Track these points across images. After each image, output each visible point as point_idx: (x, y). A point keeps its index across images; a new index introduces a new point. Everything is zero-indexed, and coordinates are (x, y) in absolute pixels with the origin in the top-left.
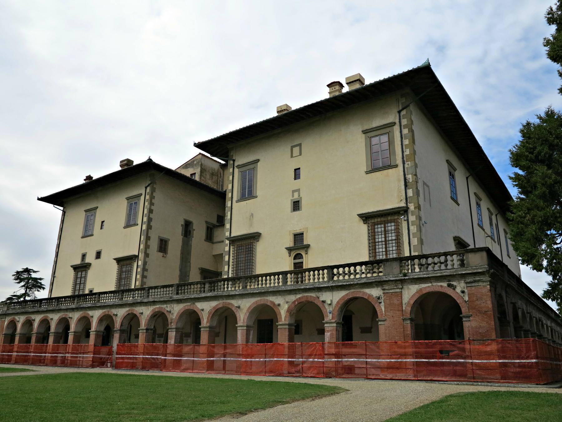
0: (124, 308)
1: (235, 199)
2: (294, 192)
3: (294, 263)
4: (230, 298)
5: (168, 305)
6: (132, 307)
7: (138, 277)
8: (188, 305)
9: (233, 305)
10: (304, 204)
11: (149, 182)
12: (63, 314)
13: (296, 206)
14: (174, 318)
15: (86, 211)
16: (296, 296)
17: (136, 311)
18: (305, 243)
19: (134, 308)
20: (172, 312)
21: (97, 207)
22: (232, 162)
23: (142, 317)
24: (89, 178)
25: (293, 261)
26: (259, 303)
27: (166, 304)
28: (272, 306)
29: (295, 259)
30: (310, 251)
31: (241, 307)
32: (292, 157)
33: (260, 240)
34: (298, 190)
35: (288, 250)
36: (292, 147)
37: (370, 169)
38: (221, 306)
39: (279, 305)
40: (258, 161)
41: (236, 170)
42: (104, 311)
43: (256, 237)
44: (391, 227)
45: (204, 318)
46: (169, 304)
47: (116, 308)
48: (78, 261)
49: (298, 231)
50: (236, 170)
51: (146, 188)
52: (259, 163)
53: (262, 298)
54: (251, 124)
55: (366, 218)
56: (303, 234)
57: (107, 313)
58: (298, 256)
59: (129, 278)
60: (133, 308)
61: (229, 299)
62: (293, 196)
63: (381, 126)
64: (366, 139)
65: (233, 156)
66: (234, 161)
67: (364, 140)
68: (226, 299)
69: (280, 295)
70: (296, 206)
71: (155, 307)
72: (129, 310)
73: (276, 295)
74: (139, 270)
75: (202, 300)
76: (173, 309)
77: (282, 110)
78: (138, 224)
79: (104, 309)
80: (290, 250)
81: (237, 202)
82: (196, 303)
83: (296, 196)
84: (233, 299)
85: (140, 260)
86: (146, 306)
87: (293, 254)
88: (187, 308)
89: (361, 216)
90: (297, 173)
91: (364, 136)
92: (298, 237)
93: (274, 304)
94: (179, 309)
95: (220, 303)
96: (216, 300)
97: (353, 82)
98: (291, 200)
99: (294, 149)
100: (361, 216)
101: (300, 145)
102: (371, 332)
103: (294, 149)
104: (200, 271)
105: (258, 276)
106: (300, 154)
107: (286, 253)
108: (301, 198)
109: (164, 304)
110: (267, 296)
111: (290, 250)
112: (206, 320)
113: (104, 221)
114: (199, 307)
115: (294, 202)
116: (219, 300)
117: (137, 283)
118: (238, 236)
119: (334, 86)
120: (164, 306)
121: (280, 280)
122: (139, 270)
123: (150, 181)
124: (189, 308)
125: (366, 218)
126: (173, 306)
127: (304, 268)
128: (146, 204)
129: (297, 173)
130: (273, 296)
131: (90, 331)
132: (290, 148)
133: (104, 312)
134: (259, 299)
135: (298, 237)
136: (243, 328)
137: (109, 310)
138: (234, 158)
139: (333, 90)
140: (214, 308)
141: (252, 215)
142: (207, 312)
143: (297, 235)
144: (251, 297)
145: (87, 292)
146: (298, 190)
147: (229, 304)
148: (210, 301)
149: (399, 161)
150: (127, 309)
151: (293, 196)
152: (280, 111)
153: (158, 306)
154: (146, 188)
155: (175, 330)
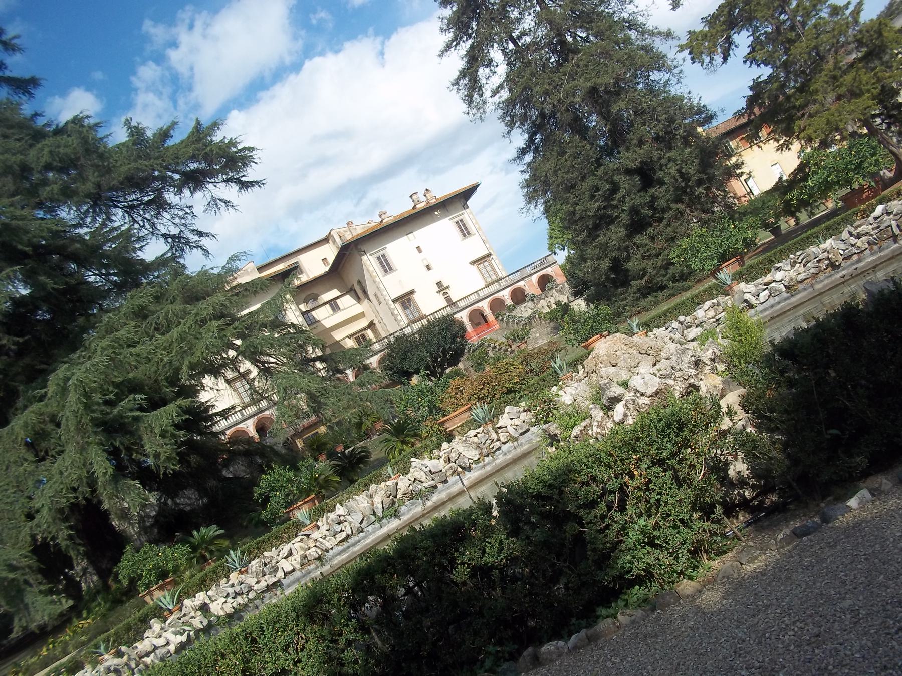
1: (380, 275)
2: (423, 260)
10: (432, 265)
13: (428, 268)
18: (445, 286)
32: (410, 240)
43: (412, 292)
44: (486, 264)
55: (473, 263)
70: (428, 268)
80: (438, 292)
81: (384, 276)
89: (471, 264)
92: (439, 284)
100: (471, 264)
125: (473, 263)
135: (439, 284)
141: (400, 281)
146: (425, 259)
149: (476, 232)
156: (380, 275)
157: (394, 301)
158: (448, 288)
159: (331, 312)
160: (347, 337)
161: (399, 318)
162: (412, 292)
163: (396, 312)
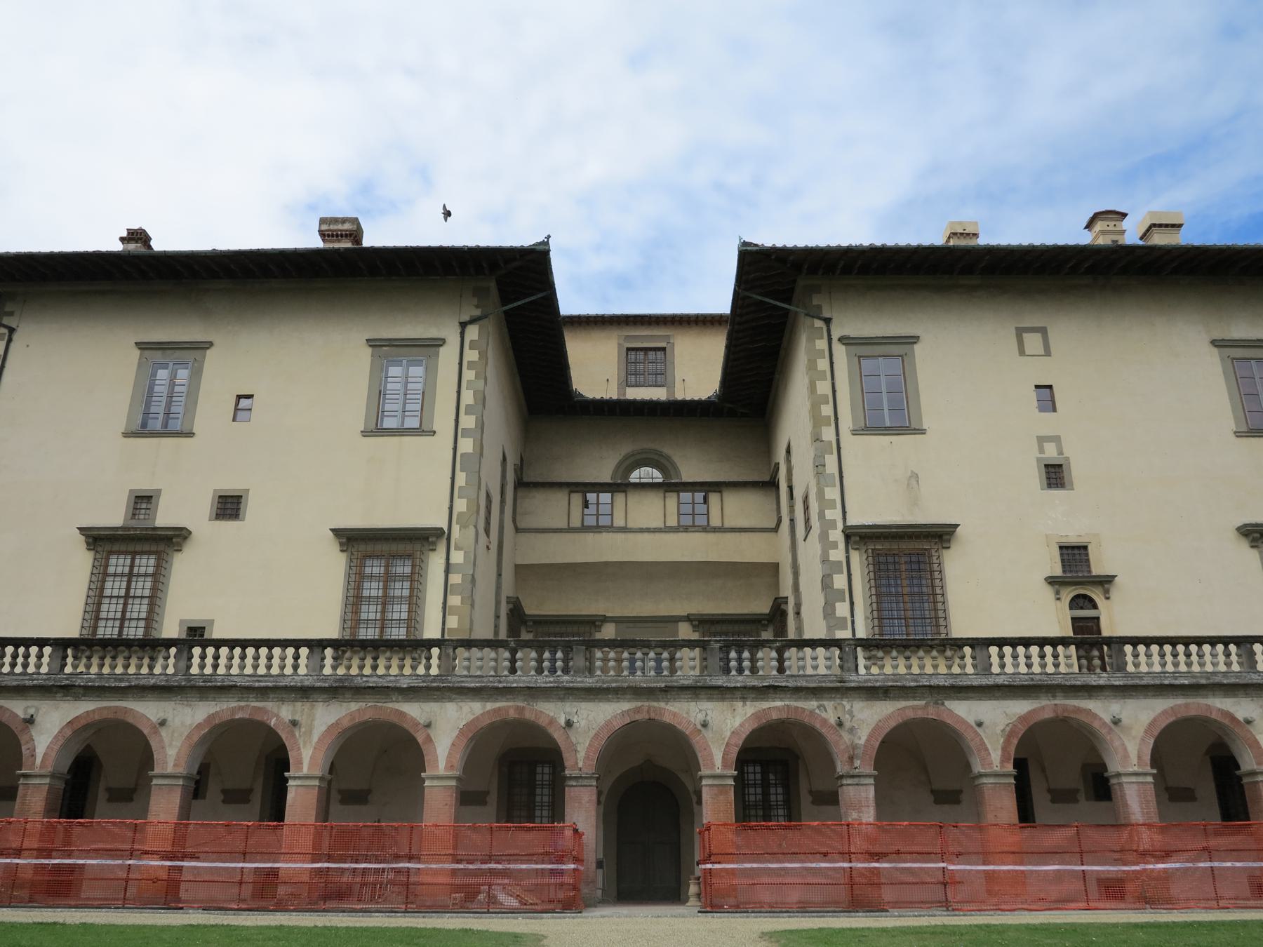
0: (609, 700)
1: (846, 423)
2: (1042, 440)
3: (1073, 619)
4: (1080, 694)
5: (826, 703)
6: (648, 700)
7: (454, 600)
8: (913, 708)
9: (1095, 716)
10: (1077, 471)
11: (477, 312)
12: (234, 704)
13: (1055, 475)
14: (862, 742)
15: (142, 346)
16: (1040, 703)
17: (675, 715)
18: (1097, 570)
19: (662, 705)
20: (847, 725)
21: (211, 344)
22: (819, 324)
23: (708, 734)
24: (138, 236)
25: (1068, 614)
26: (1183, 714)
27: (821, 698)
28: (1226, 722)
29: (1071, 608)
30: (1114, 594)
31: (1125, 721)
32: (1022, 352)
33: (952, 546)
34: (1056, 439)
35: (1050, 583)
36: (1020, 332)
37: (1244, 429)
38: (1048, 714)
39: (1248, 722)
40: (913, 340)
41: (839, 350)
42: (490, 706)
43: (942, 535)
45: (989, 746)
46: (831, 699)
47: (562, 699)
48: (114, 516)
49: (1073, 539)
50: (839, 350)
51: (463, 325)
52: (916, 347)
53: (1190, 700)
54: (1012, 244)
56: (1085, 548)
57: (512, 714)
58: (1081, 601)
59: (415, 601)
60: (655, 704)
61: (1076, 697)
62: (1041, 450)
63: (1252, 340)
64: (1222, 360)
65: (819, 307)
66: (828, 321)
67: (1217, 360)
68: (1066, 697)
69: (1247, 695)
70: (1055, 475)
71: (765, 705)
72: (637, 710)
73: (1235, 696)
74: (455, 579)
75: (970, 695)
76: (853, 717)
77: (968, 234)
78: (435, 432)
79: (496, 700)
80: (1052, 581)
81: (855, 432)
82: (947, 703)
83: (1051, 453)
84: (1090, 697)
85: (457, 548)
86: (723, 699)
87: (1068, 594)
88: (910, 714)
90: (1046, 395)
91: (1215, 350)
92: (1074, 554)
93: (1233, 718)
94: (876, 718)
95: (1043, 708)
96: (1025, 697)
97: (1167, 226)
98: (1038, 460)
99: (1025, 335)
101: (1043, 331)
102: (958, 802)
103: (1025, 335)
104: (511, 606)
105: (959, 644)
106: (1048, 353)
107: (1049, 592)
108: (1067, 459)
109: (806, 699)
110: (1206, 696)
111: (1052, 581)
112: (999, 752)
113: (250, 397)
114: (960, 714)
115: (1047, 466)
116: (1037, 698)
117: (453, 622)
118: (890, 526)
119: (1111, 219)
120: (812, 704)
121: (1234, 658)
122: (455, 579)
123: (477, 307)
124: (920, 714)
126: (848, 707)
127: (1106, 632)
128: (469, 375)
129: (1046, 395)
130: (1226, 695)
131: (286, 774)
132: (1014, 331)
133: (495, 711)
134: (1180, 701)
136: (1141, 779)
137: (521, 704)
138: (826, 314)
139: (1109, 229)
140: (1022, 719)
141: (915, 476)
142: (999, 732)
143: (1067, 548)
144: (1154, 696)
145: (170, 629)
146: (1056, 439)
147: (1079, 710)
148: (1004, 697)
150: (624, 706)
151: (1041, 450)
152: (961, 234)
153: (779, 704)
154: (463, 325)
155: (872, 781)
156: (846, 423)
157: (857, 536)
158: (1105, 582)
159: (672, 522)
160: (688, 618)
161: (842, 609)
162: (942, 535)
163: (840, 582)
